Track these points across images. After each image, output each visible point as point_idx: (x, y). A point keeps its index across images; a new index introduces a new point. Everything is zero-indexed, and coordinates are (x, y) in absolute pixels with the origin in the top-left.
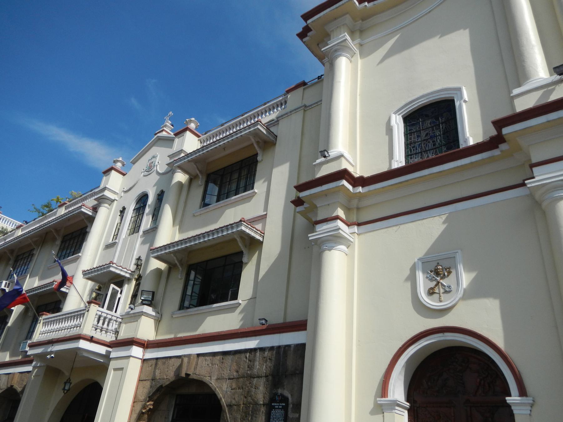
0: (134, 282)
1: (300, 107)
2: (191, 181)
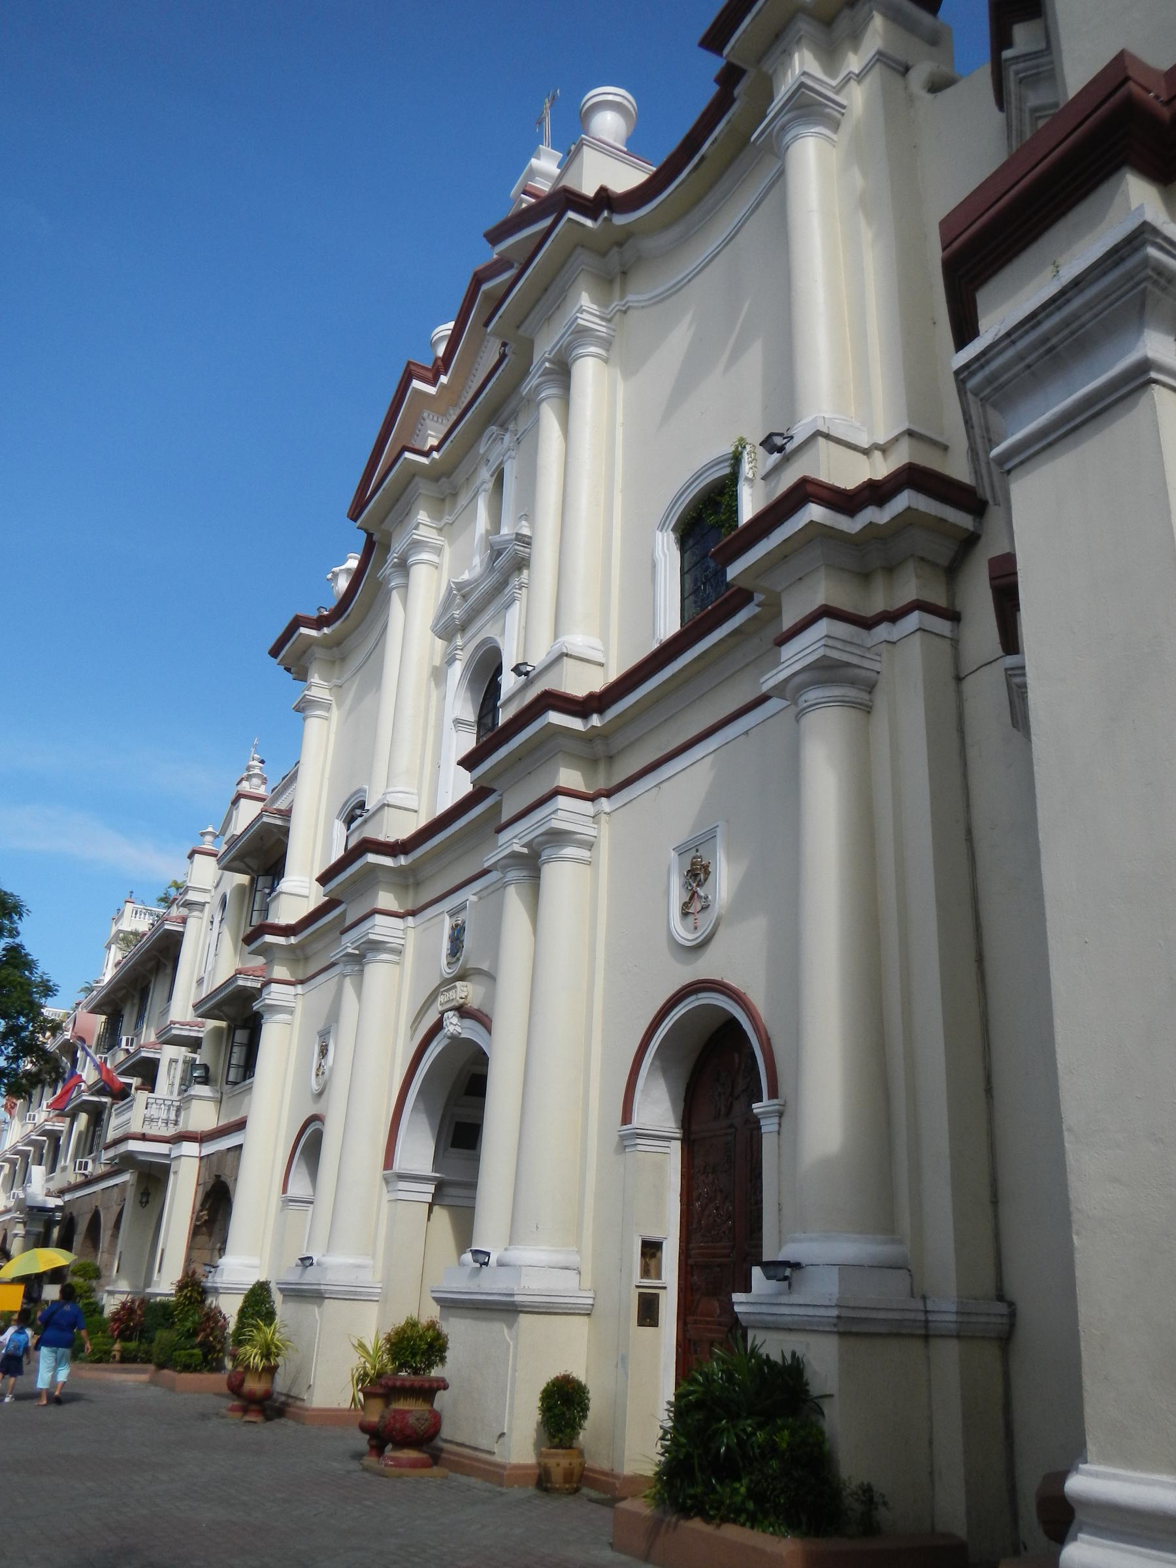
2: (253, 881)
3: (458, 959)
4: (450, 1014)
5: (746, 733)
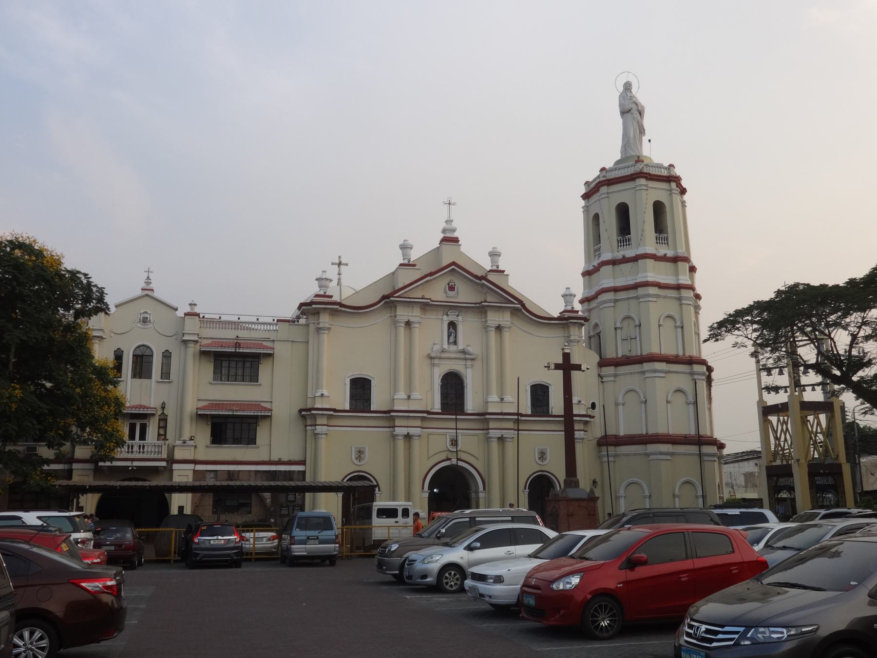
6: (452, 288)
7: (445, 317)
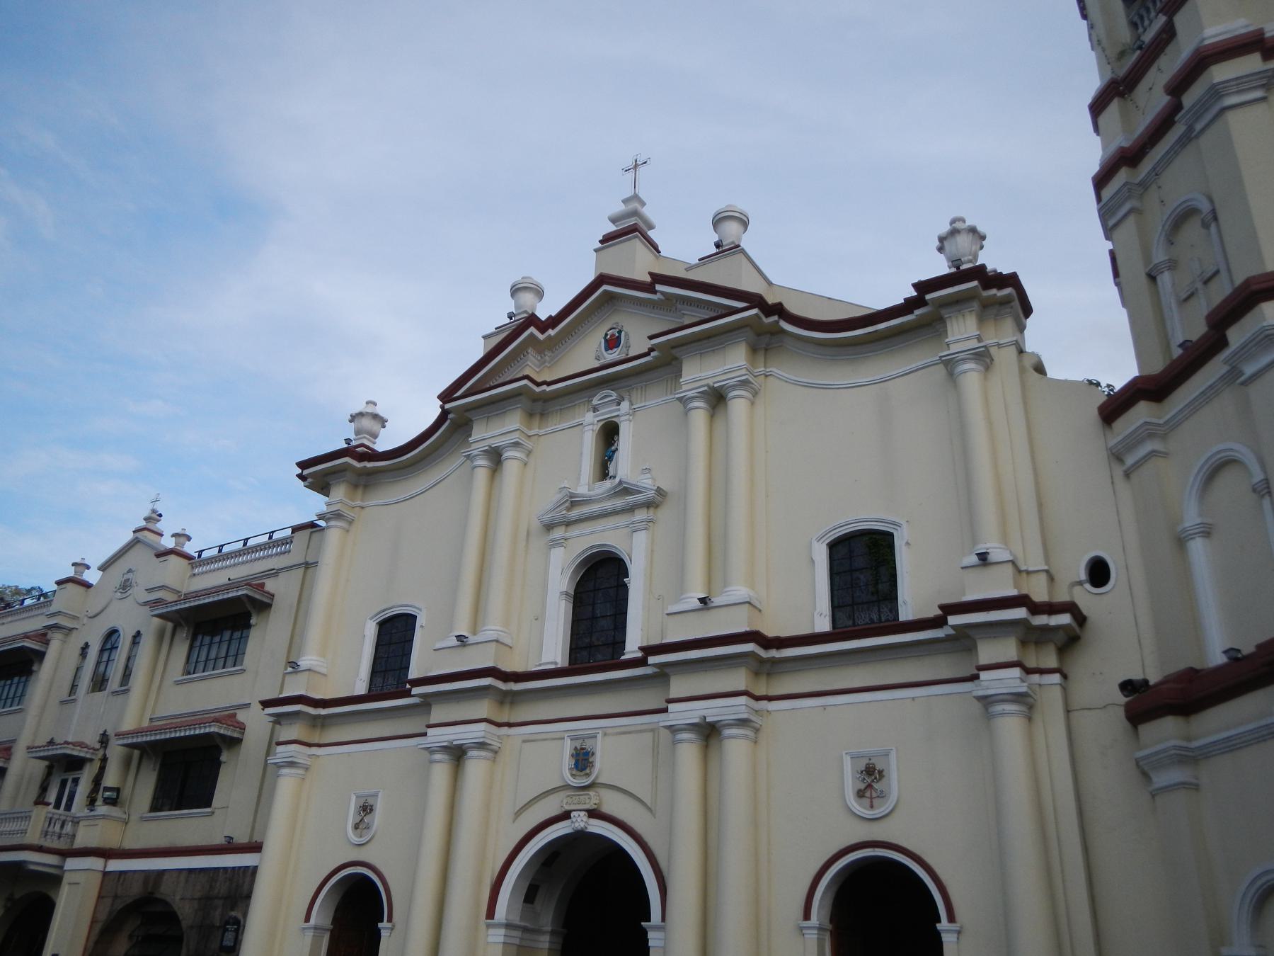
0: (97, 765)
1: (300, 564)
3: (588, 775)
4: (582, 814)
5: (913, 699)
6: (612, 343)
7: (589, 417)
